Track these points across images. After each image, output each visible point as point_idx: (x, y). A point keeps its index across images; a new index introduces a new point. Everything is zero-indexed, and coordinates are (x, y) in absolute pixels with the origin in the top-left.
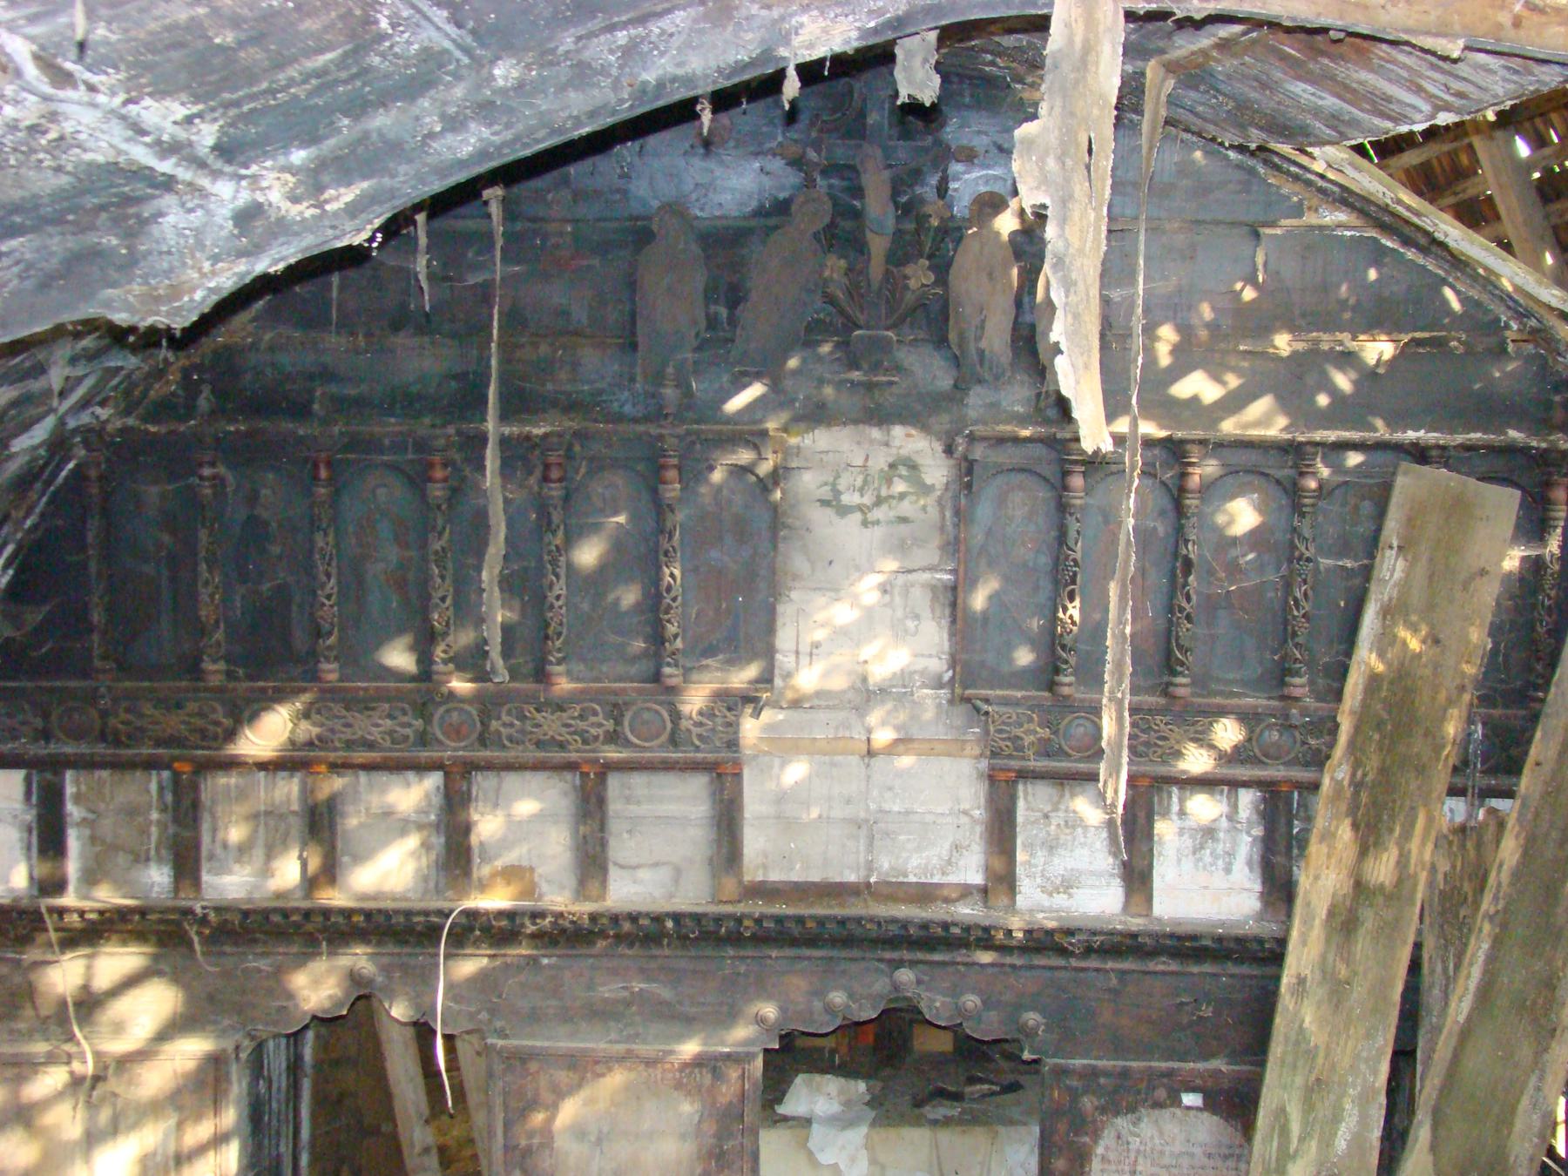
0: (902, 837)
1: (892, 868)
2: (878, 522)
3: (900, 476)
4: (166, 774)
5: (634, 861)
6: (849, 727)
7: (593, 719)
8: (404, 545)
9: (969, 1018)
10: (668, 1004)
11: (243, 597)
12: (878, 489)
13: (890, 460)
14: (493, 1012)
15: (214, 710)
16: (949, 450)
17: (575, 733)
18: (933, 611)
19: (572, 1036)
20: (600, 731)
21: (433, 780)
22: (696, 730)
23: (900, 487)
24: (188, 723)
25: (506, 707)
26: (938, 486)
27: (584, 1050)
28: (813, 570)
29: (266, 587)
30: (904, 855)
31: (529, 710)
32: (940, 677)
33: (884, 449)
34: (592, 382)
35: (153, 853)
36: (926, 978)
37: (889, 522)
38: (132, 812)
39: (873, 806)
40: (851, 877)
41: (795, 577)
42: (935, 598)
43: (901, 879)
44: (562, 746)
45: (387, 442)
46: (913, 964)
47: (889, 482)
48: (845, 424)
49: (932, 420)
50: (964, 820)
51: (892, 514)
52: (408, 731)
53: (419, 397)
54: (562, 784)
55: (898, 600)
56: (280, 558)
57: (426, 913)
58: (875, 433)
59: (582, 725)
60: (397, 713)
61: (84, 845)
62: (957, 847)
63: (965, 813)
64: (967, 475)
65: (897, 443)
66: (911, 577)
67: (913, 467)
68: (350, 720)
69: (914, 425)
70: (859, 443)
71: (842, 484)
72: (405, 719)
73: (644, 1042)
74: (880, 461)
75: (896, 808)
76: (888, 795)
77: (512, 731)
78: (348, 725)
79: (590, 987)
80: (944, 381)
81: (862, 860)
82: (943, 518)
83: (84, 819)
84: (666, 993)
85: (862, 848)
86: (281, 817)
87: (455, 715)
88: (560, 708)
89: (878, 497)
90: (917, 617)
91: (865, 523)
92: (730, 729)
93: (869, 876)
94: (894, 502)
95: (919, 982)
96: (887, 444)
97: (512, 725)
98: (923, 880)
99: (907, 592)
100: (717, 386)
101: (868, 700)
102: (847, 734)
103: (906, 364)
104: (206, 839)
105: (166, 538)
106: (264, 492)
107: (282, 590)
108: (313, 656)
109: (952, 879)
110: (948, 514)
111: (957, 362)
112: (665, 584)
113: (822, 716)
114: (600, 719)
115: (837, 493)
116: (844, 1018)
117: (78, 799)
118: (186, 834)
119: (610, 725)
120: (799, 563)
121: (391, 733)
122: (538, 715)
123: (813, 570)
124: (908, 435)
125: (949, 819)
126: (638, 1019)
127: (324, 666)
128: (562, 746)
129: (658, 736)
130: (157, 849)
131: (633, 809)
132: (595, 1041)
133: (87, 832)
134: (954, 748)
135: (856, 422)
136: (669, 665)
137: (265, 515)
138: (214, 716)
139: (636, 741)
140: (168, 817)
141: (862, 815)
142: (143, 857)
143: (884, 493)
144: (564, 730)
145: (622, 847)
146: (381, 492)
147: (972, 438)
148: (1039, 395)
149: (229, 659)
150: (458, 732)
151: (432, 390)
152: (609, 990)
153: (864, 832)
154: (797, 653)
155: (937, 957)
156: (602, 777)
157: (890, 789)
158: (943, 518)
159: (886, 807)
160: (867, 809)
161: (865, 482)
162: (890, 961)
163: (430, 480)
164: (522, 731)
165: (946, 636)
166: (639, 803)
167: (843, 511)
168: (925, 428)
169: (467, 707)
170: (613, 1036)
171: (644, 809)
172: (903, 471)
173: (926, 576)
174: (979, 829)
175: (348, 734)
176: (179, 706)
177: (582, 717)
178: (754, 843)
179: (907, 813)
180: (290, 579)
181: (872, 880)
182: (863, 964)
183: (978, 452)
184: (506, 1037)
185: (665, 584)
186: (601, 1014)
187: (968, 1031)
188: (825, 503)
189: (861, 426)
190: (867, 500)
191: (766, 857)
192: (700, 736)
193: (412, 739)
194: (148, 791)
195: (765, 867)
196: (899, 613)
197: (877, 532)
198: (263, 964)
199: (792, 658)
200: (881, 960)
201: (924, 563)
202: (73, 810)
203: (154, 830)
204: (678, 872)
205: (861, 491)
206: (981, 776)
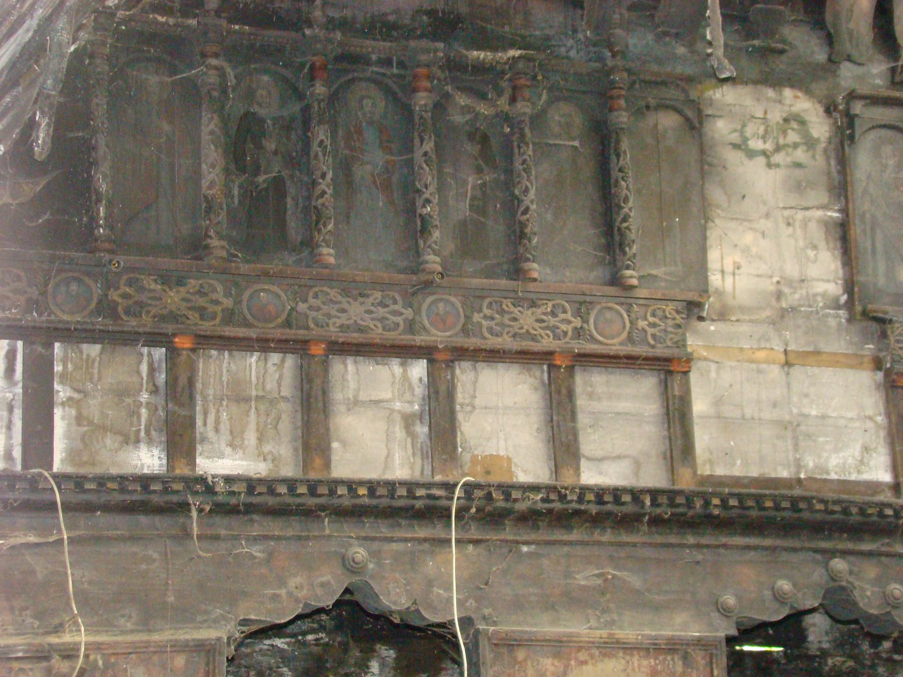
0: (821, 439)
1: (816, 467)
2: (777, 166)
3: (793, 129)
4: (159, 353)
5: (599, 453)
6: (768, 340)
7: (562, 316)
8: (390, 151)
9: (895, 607)
10: (637, 592)
11: (240, 187)
12: (776, 138)
13: (784, 115)
14: (478, 600)
15: (215, 290)
16: (829, 110)
17: (547, 328)
18: (827, 243)
19: (555, 622)
20: (569, 328)
21: (419, 369)
22: (650, 331)
23: (793, 137)
24: (188, 300)
25: (487, 301)
26: (823, 139)
27: (571, 635)
28: (729, 202)
29: (261, 179)
30: (825, 455)
31: (507, 305)
32: (837, 299)
33: (779, 106)
34: (542, 29)
35: (143, 434)
36: (855, 569)
37: (787, 166)
38: (121, 393)
39: (795, 411)
40: (784, 474)
41: (719, 207)
42: (827, 231)
43: (825, 476)
44: (534, 338)
45: (374, 57)
46: (844, 553)
47: (785, 133)
48: (747, 83)
49: (814, 86)
50: (869, 425)
51: (789, 159)
52: (399, 319)
53: (394, 26)
54: (531, 380)
55: (799, 232)
56: (276, 153)
57: (429, 486)
58: (770, 93)
59: (552, 321)
60: (388, 301)
61: (69, 425)
62: (866, 449)
63: (870, 418)
64: (846, 133)
65: (788, 102)
66: (808, 213)
67: (802, 123)
68: (345, 306)
69: (800, 89)
70: (758, 100)
71: (749, 130)
72: (396, 307)
73: (620, 628)
74: (776, 116)
75: (814, 413)
76: (805, 401)
77: (492, 323)
78: (344, 311)
79: (568, 575)
80: (821, 56)
81: (791, 458)
82: (829, 165)
83: (70, 399)
84: (635, 581)
85: (790, 447)
86: (272, 402)
87: (441, 305)
88: (533, 304)
89: (777, 144)
90: (815, 247)
91: (769, 165)
92: (679, 331)
93: (798, 472)
94: (790, 150)
95: (851, 572)
96: (780, 102)
97: (492, 318)
98: (842, 478)
99: (806, 225)
100: (644, 42)
101: (782, 317)
102: (768, 346)
103: (790, 39)
104: (199, 422)
105: (166, 127)
106: (260, 92)
107: (278, 184)
108: (309, 244)
109: (866, 476)
110: (833, 162)
111: (830, 40)
112: (623, 195)
113: (744, 328)
114: (569, 316)
115: (745, 140)
116: (792, 607)
117: (64, 378)
118: (184, 412)
119: (577, 322)
120: (716, 194)
121: (382, 319)
122: (516, 310)
123: (729, 202)
124: (796, 97)
125: (857, 424)
126: (612, 605)
127: (325, 250)
128: (534, 338)
129: (619, 335)
130: (148, 432)
131: (596, 406)
132: (577, 626)
133: (74, 412)
134: (852, 362)
135: (756, 82)
136: (628, 267)
137: (262, 112)
138: (214, 296)
139: (601, 339)
140: (160, 400)
141: (787, 417)
142: (132, 437)
143: (781, 142)
144: (537, 325)
145: (590, 442)
146: (367, 103)
147: (852, 96)
148: (893, 70)
149: (232, 241)
150: (444, 322)
151: (407, 22)
152: (585, 577)
153: (789, 433)
154: (723, 272)
155: (866, 547)
156: (571, 369)
157: (806, 396)
158: (829, 165)
159: (806, 411)
160: (791, 413)
161: (766, 131)
162: (823, 551)
163: (415, 90)
164: (503, 325)
165: (839, 264)
166: (599, 399)
167: (751, 154)
168: (808, 92)
169: (453, 299)
170: (593, 623)
171: (603, 405)
172: (794, 125)
173: (820, 213)
174: (882, 434)
175: (343, 320)
176: (180, 282)
177: (553, 314)
178: (703, 440)
179: (824, 417)
180: (285, 173)
181: (802, 476)
182: (802, 555)
183: (858, 108)
184: (495, 623)
185: (623, 195)
186: (576, 601)
187: (897, 619)
188: (736, 146)
189: (759, 87)
190: (769, 146)
191: (711, 453)
192: (654, 336)
193: (402, 327)
194: (138, 372)
195: (711, 462)
196: (801, 243)
197: (778, 175)
198: (257, 551)
199: (719, 276)
200: (816, 551)
201: (817, 203)
202: (61, 391)
203: (144, 411)
204: (637, 465)
205: (764, 138)
206: (878, 387)
